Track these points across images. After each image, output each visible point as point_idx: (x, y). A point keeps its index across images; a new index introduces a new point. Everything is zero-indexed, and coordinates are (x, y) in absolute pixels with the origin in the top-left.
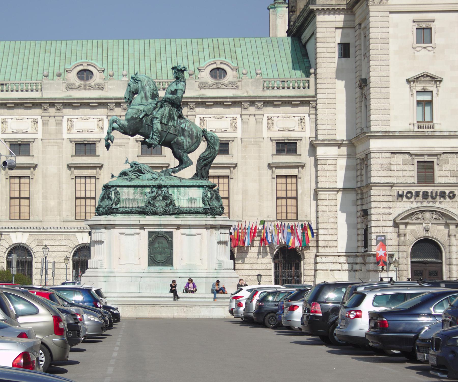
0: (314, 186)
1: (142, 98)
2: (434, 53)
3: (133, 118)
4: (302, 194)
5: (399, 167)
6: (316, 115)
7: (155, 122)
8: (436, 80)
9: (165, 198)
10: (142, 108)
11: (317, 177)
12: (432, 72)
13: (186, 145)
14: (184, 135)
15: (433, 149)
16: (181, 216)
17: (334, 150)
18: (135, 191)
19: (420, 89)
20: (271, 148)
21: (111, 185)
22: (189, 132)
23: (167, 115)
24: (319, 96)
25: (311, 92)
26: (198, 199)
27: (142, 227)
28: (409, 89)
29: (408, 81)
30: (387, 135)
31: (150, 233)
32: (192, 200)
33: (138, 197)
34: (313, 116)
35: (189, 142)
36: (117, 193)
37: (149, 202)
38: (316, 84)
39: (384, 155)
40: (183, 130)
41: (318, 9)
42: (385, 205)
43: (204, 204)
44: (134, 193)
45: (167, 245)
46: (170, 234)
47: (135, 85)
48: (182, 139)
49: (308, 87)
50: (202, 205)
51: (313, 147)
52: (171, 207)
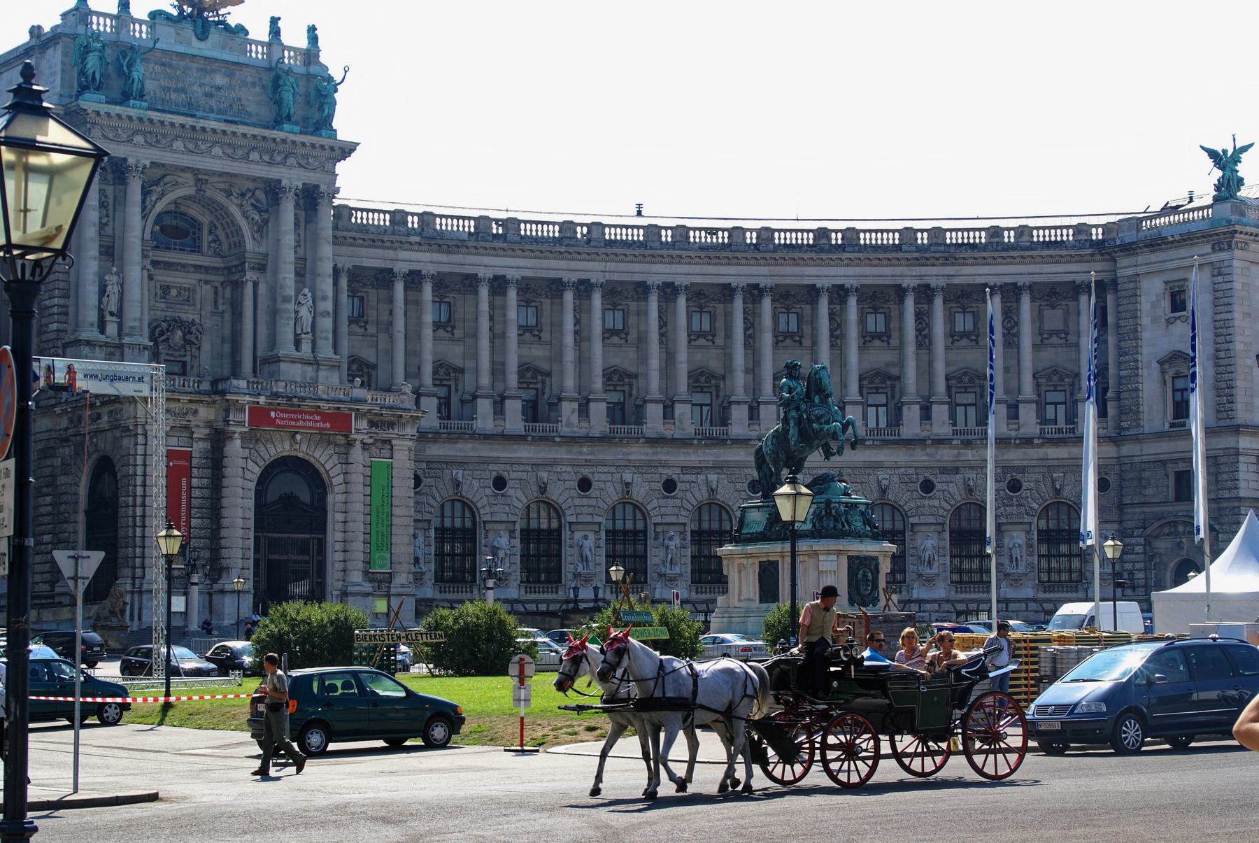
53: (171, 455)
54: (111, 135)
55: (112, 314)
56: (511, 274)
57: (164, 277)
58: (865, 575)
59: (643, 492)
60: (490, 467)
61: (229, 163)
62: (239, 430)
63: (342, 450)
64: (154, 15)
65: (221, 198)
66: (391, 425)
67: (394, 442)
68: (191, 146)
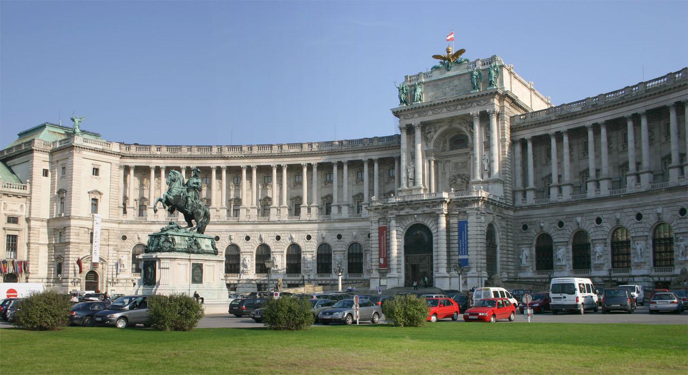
0: (26, 241)
3: (176, 195)
4: (20, 246)
5: (82, 235)
6: (30, 204)
7: (189, 199)
8: (100, 193)
9: (197, 244)
10: (180, 190)
11: (29, 237)
12: (99, 190)
14: (201, 209)
16: (205, 255)
17: (39, 223)
19: (93, 197)
20: (5, 220)
24: (33, 194)
25: (27, 192)
27: (190, 260)
28: (88, 197)
29: (89, 193)
30: (80, 218)
31: (193, 264)
32: (207, 246)
33: (183, 242)
34: (28, 205)
36: (173, 239)
37: (190, 246)
38: (31, 188)
39: (77, 228)
40: (200, 206)
41: (36, 150)
42: (76, 253)
43: (213, 248)
45: (200, 271)
46: (202, 264)
49: (26, 189)
50: (213, 250)
51: (28, 220)
53: (379, 228)
54: (407, 117)
55: (411, 179)
56: (600, 121)
57: (454, 160)
58: (148, 271)
59: (669, 217)
60: (594, 214)
61: (449, 113)
62: (391, 216)
63: (436, 219)
64: (432, 69)
65: (458, 126)
66: (467, 205)
67: (467, 212)
68: (435, 112)
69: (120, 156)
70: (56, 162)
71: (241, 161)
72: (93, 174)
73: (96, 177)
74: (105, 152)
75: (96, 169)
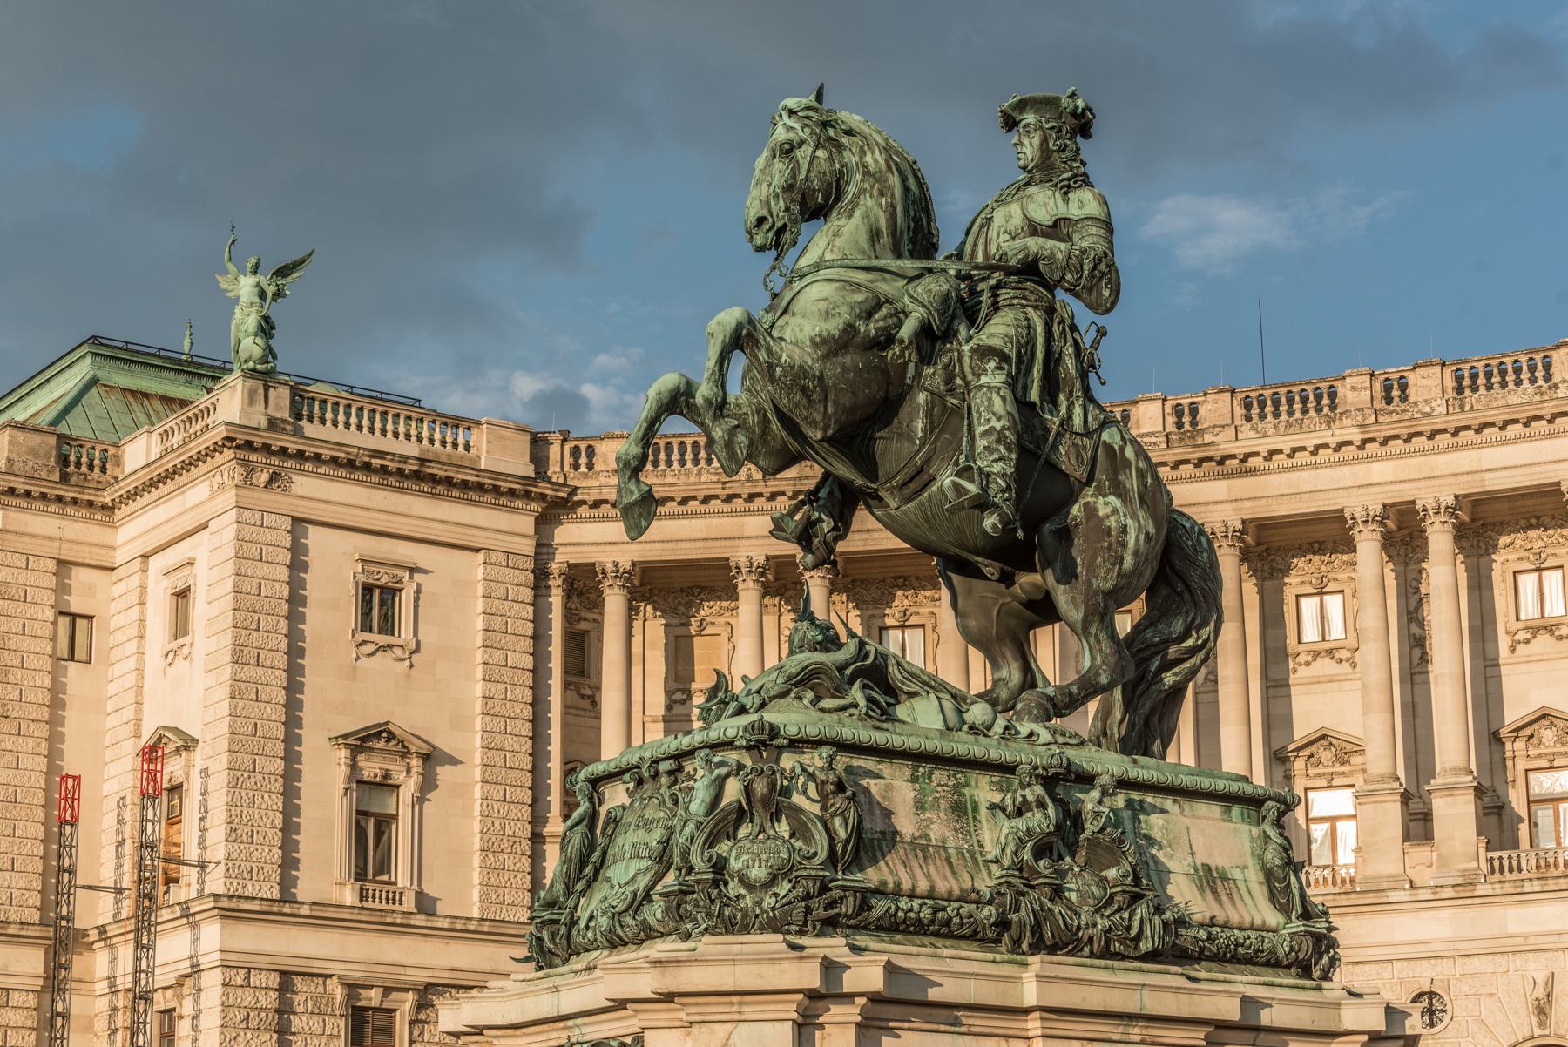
1: (874, 235)
2: (411, 666)
13: (1136, 553)
15: (402, 970)
18: (922, 791)
21: (792, 731)
22: (1141, 475)
23: (1040, 355)
26: (1237, 874)
32: (1211, 879)
33: (939, 829)
35: (1147, 534)
40: (1116, 460)
44: (919, 806)
47: (821, 153)
48: (1115, 512)
50: (1273, 918)
52: (1141, 910)
69: (536, 507)
70: (137, 565)
71: (1346, 475)
72: (366, 627)
73: (384, 639)
74: (434, 480)
75: (383, 589)
